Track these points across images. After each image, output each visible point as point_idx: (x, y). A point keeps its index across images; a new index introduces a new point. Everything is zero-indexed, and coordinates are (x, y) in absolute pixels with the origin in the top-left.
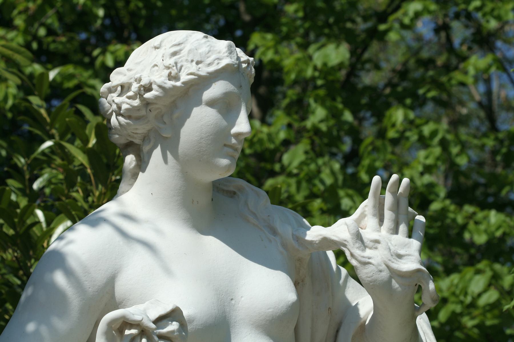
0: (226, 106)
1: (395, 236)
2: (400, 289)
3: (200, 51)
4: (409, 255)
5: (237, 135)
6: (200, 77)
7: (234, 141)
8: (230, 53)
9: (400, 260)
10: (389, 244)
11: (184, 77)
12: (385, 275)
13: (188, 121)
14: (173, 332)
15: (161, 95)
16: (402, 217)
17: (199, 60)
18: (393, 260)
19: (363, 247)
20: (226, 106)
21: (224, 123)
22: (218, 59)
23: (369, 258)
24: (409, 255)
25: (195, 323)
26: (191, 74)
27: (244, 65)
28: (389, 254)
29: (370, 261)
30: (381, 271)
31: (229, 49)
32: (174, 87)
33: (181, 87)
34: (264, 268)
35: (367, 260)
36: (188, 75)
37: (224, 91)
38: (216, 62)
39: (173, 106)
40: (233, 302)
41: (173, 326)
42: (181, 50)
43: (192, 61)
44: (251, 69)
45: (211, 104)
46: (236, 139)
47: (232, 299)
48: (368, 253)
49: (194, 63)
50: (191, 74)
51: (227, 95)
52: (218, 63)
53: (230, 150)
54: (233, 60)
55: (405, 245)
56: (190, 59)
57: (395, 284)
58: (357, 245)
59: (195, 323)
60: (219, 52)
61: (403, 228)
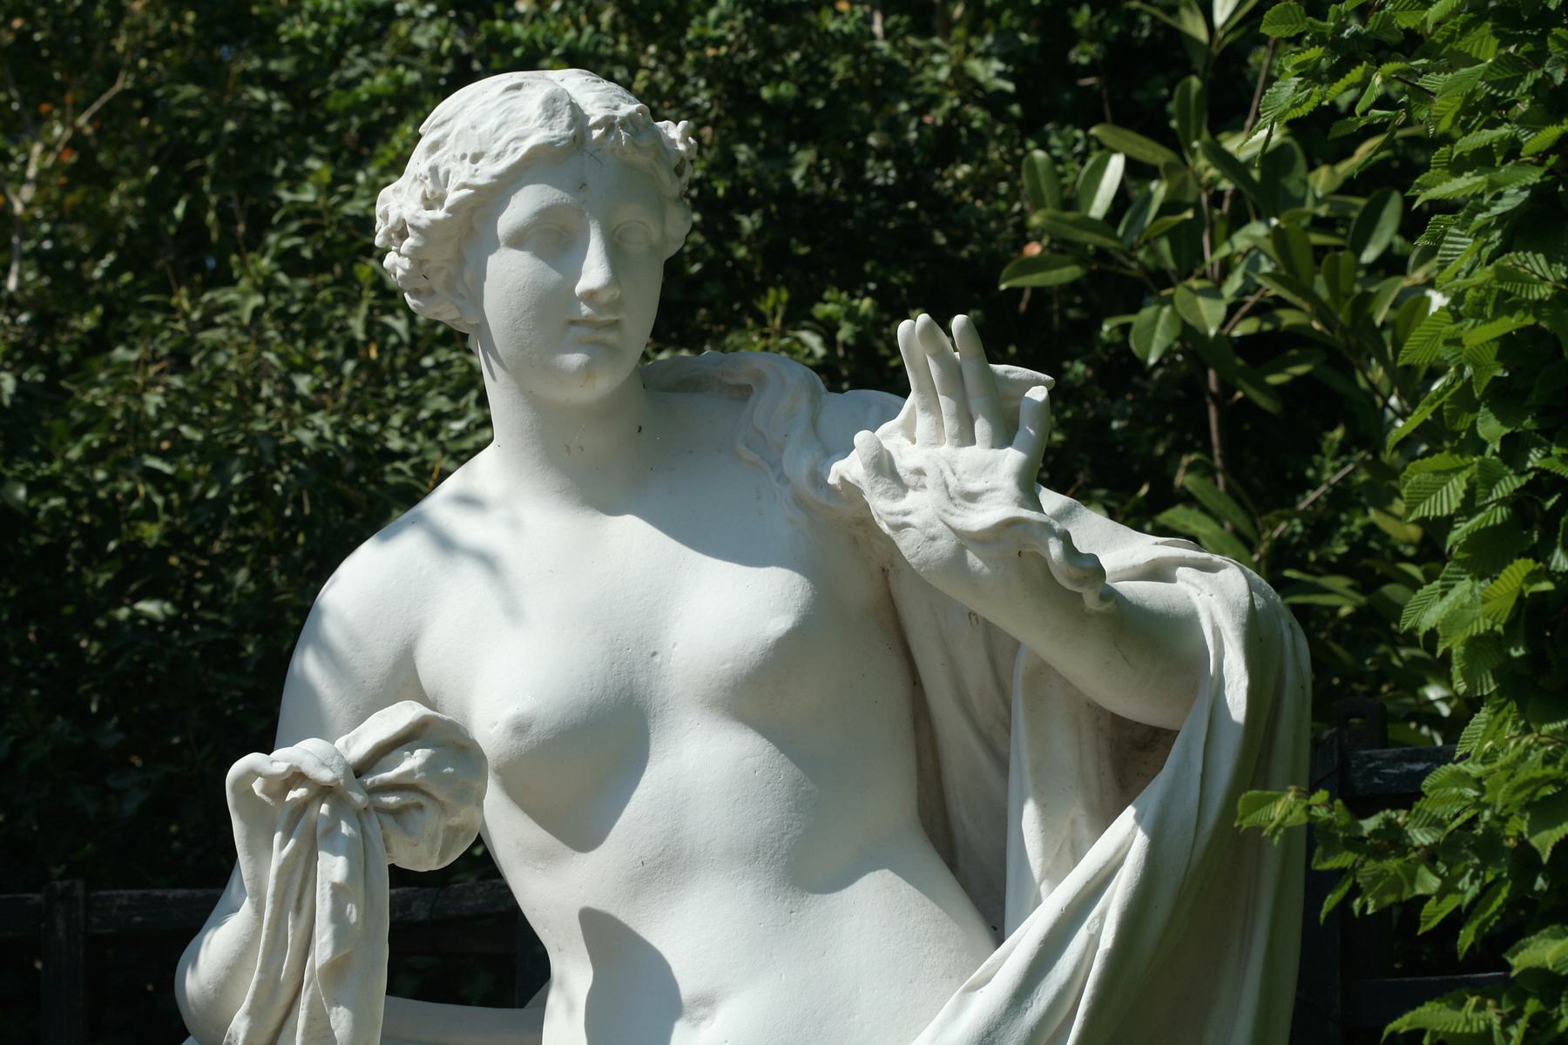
0: (552, 239)
1: (968, 450)
2: (986, 570)
3: (481, 130)
4: (992, 490)
5: (590, 296)
6: (478, 189)
7: (585, 310)
8: (550, 118)
9: (972, 506)
10: (948, 473)
11: (453, 196)
12: (945, 545)
13: (487, 285)
14: (411, 773)
15: (419, 244)
16: (975, 403)
17: (477, 151)
18: (953, 509)
19: (895, 488)
20: (552, 239)
21: (554, 276)
22: (519, 138)
23: (906, 514)
24: (992, 490)
25: (534, 730)
26: (464, 186)
27: (596, 133)
28: (944, 496)
29: (907, 519)
30: (933, 539)
31: (546, 109)
32: (434, 222)
33: (446, 219)
34: (727, 564)
35: (901, 519)
36: (458, 189)
37: (537, 208)
38: (512, 146)
39: (460, 260)
40: (657, 659)
41: (413, 761)
42: (446, 136)
43: (464, 157)
44: (618, 136)
45: (518, 240)
46: (589, 305)
47: (654, 654)
48: (911, 500)
49: (467, 160)
50: (464, 186)
51: (544, 216)
52: (515, 150)
53: (583, 332)
54: (556, 132)
55: (985, 468)
56: (459, 155)
57: (974, 561)
58: (879, 488)
59: (534, 730)
60: (527, 121)
61: (981, 427)
